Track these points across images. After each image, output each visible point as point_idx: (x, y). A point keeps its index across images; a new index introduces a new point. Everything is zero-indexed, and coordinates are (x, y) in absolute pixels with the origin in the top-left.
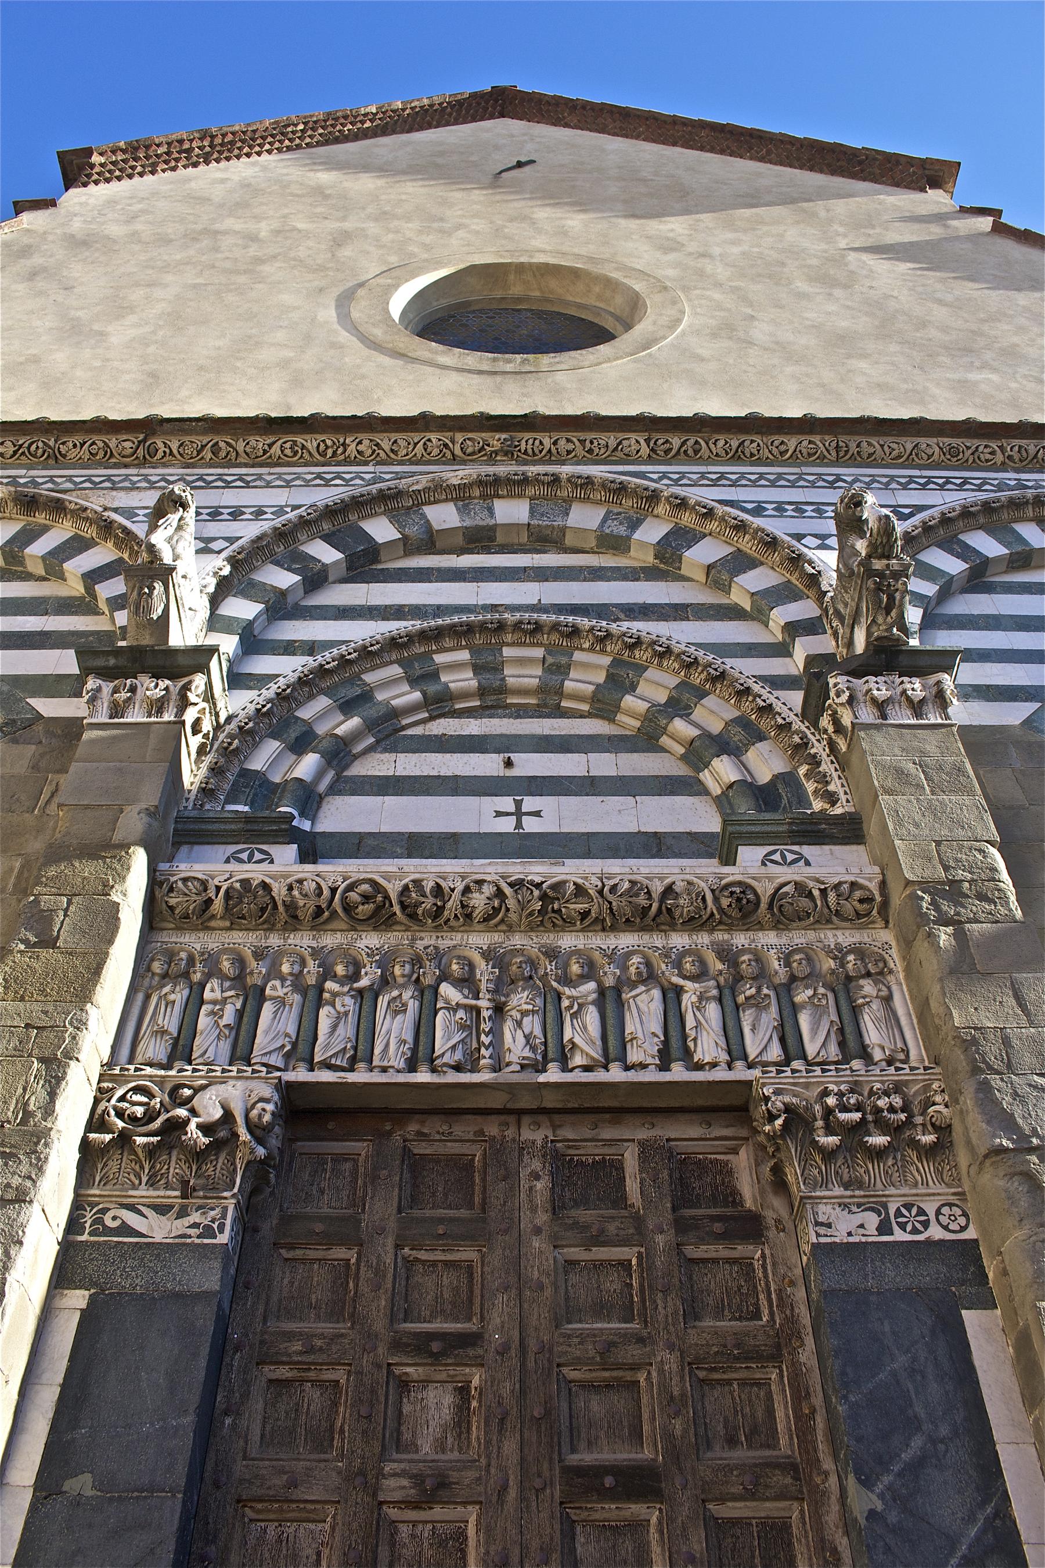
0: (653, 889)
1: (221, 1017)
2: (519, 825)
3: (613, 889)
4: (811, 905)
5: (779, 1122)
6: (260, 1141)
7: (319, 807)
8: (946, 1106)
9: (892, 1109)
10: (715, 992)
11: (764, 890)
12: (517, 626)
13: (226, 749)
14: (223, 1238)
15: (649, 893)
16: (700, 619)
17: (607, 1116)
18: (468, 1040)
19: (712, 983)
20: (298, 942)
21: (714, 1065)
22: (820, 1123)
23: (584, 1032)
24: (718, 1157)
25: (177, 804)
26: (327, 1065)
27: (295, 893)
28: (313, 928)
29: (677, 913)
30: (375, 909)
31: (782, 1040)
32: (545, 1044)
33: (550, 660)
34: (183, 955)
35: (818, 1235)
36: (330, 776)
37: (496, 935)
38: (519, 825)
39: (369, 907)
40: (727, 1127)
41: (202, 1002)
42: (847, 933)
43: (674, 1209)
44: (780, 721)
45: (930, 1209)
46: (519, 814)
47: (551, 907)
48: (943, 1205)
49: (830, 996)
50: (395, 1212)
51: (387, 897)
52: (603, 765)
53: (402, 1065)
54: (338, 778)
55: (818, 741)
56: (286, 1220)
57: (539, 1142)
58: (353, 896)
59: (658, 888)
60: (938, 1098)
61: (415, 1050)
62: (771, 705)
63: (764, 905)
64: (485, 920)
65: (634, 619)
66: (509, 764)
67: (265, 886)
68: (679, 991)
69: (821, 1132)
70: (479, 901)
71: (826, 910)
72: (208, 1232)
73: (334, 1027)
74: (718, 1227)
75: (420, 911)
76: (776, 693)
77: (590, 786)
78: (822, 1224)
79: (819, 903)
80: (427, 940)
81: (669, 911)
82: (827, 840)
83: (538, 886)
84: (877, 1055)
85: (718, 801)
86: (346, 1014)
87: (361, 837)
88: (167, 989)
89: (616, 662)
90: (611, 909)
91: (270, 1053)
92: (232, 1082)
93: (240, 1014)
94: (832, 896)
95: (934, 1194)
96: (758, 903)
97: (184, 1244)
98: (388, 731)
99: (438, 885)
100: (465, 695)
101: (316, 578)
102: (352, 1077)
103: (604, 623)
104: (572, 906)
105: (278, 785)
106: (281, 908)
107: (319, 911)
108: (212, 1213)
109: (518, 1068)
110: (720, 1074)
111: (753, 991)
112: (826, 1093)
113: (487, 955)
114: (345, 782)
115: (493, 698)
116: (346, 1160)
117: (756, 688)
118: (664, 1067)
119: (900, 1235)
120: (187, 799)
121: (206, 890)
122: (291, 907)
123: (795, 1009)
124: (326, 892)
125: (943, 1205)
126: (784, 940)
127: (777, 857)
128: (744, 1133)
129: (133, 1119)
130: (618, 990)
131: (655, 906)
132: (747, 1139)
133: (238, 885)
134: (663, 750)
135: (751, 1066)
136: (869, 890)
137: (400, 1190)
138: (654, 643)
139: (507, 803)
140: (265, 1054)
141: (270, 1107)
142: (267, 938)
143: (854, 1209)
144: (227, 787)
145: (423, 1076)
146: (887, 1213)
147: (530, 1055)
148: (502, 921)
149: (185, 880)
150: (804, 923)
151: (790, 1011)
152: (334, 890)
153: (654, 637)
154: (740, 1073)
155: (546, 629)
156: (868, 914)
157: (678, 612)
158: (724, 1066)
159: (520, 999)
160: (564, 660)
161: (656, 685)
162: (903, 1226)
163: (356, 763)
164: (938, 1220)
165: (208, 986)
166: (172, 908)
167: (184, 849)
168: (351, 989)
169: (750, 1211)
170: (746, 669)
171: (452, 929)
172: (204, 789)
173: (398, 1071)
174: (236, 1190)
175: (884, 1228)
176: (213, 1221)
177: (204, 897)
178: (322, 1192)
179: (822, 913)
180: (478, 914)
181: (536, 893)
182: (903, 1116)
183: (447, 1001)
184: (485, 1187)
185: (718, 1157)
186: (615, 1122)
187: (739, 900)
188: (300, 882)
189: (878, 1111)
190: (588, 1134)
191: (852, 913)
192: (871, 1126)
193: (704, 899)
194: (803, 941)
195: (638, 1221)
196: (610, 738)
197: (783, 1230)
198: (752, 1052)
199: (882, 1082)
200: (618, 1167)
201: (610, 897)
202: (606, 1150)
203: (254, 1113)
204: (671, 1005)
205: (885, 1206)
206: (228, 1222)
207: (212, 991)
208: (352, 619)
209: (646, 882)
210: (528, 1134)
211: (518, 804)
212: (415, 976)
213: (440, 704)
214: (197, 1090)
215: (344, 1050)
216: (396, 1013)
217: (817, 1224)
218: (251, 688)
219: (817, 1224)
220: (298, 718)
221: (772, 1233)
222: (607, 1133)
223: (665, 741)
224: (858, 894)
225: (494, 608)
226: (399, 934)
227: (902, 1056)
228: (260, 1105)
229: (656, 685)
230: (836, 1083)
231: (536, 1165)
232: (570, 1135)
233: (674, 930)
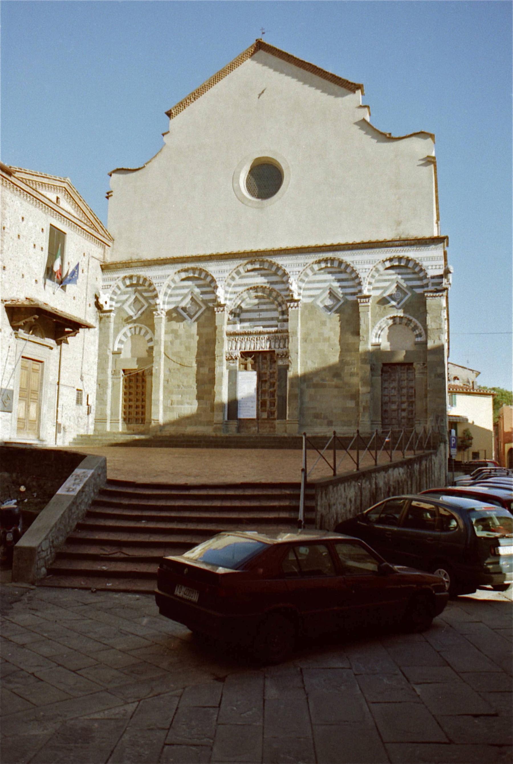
77: (267, 310)
110: (273, 350)
139: (258, 313)
161: (274, 294)
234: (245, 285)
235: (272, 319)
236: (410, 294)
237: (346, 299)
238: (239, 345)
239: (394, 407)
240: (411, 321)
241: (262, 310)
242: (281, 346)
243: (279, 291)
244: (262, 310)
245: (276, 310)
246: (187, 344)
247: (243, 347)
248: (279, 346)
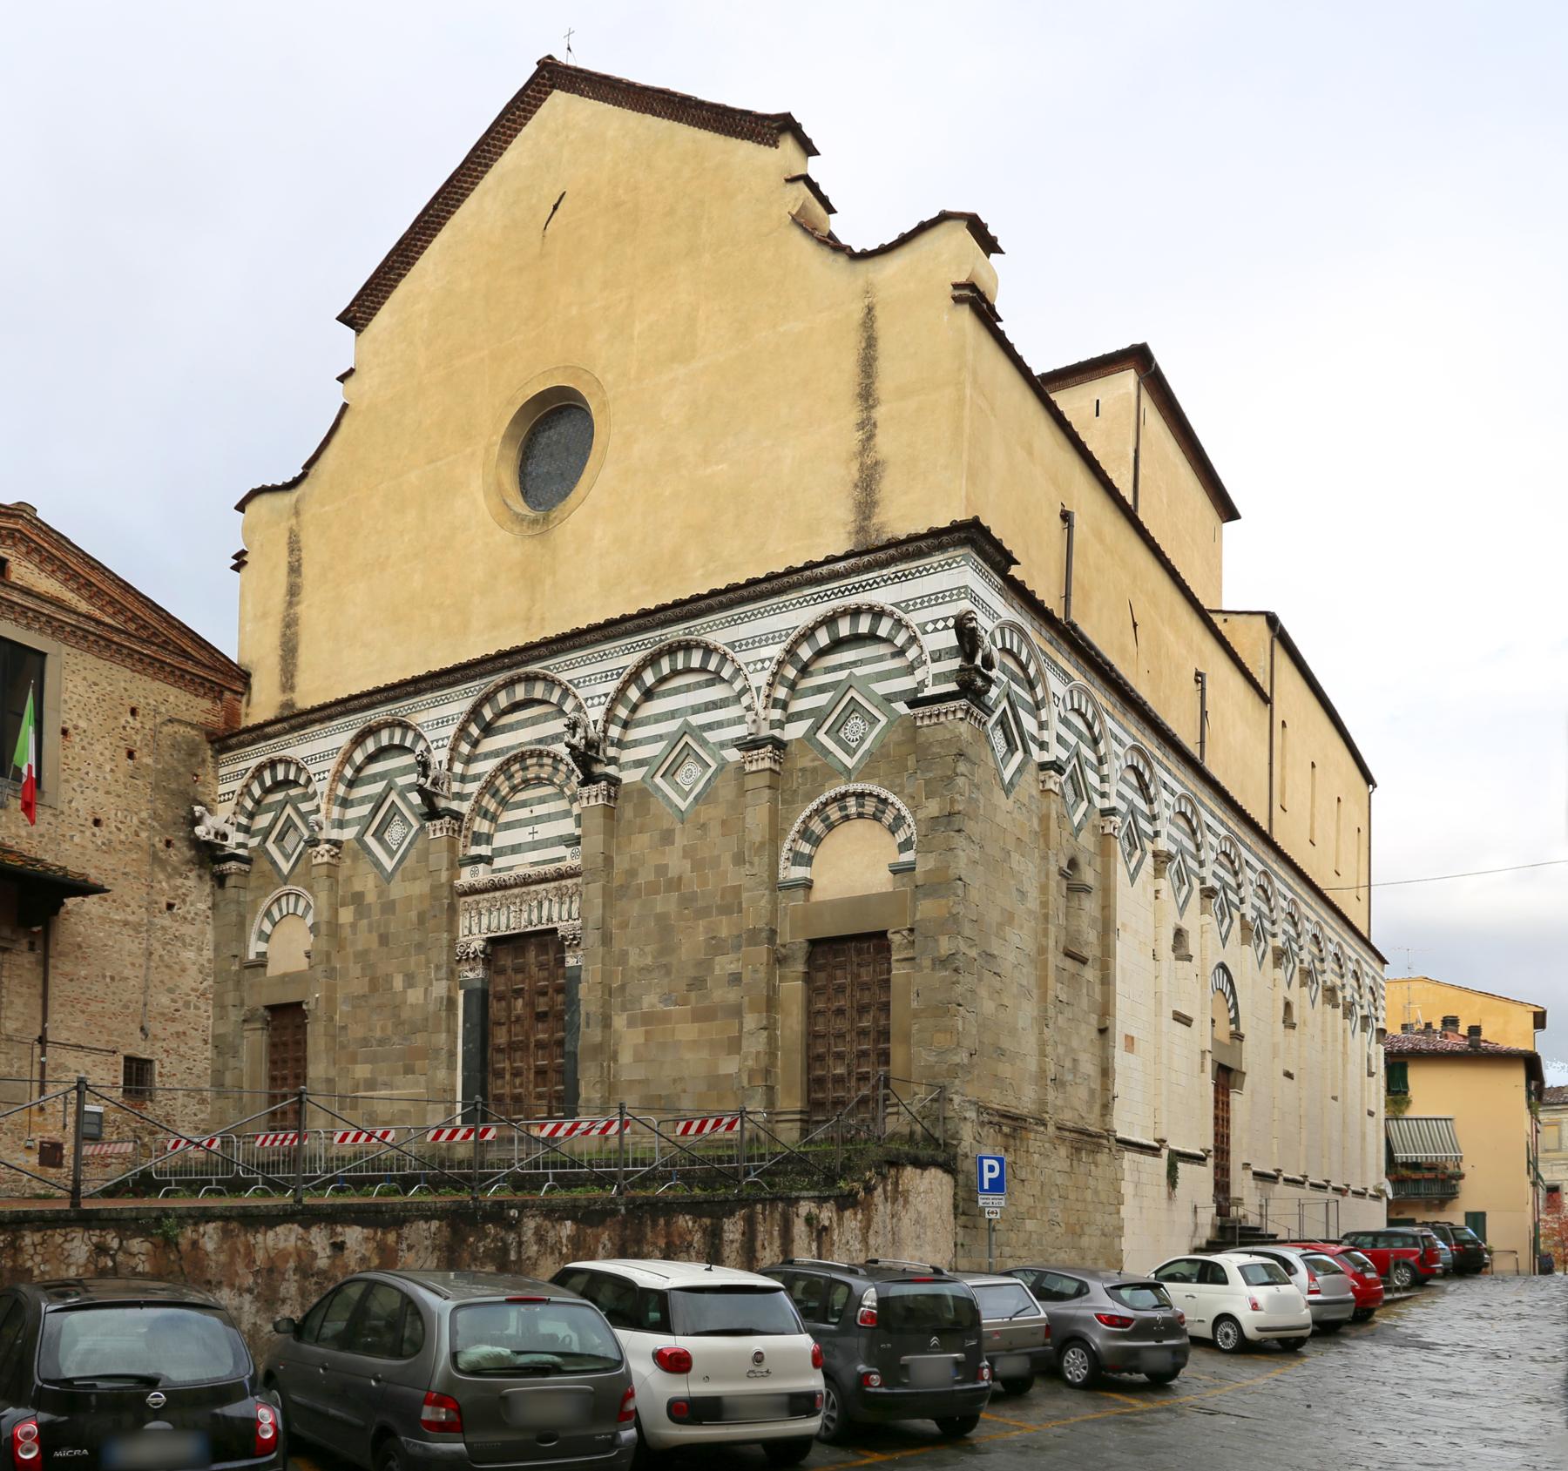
77: (549, 818)
98: (504, 803)
101: (475, 744)
213: (514, 789)
225: (521, 745)
236: (883, 721)
237: (723, 759)
239: (840, 1070)
240: (884, 801)
241: (539, 820)
244: (539, 820)
245: (567, 814)
246: (382, 930)
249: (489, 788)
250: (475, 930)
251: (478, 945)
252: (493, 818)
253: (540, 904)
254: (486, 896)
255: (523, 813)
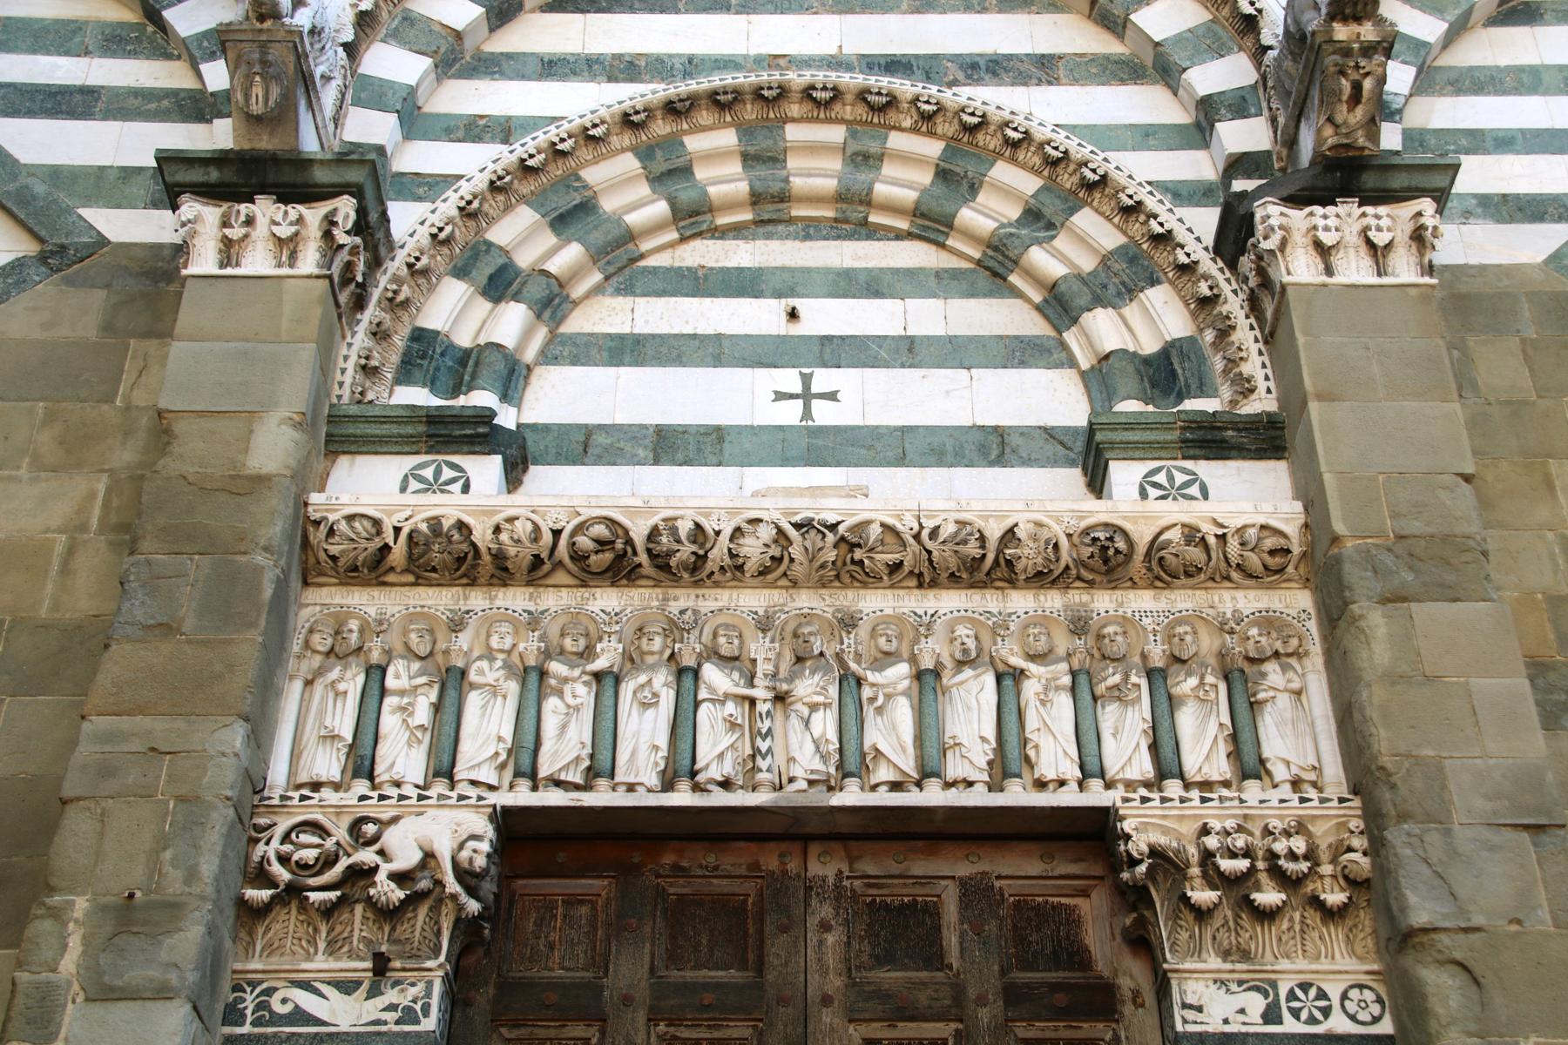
0: (987, 533)
1: (411, 714)
2: (807, 413)
3: (934, 533)
4: (1203, 557)
5: (1142, 868)
6: (472, 892)
7: (526, 384)
8: (1365, 854)
9: (1292, 856)
10: (1066, 680)
11: (1142, 535)
12: (808, 92)
13: (391, 300)
14: (430, 1024)
15: (982, 539)
16: (1075, 81)
17: (920, 844)
18: (739, 744)
19: (1064, 666)
20: (508, 604)
21: (1062, 783)
22: (1195, 871)
23: (892, 734)
24: (1064, 900)
25: (329, 396)
26: (558, 783)
27: (504, 537)
28: (529, 583)
29: (1019, 566)
30: (613, 558)
31: (1154, 748)
32: (841, 750)
33: (853, 147)
34: (354, 625)
35: (1185, 1021)
36: (542, 334)
37: (776, 592)
38: (807, 413)
39: (608, 556)
40: (1076, 861)
41: (383, 692)
42: (1252, 594)
43: (1003, 972)
44: (1183, 259)
45: (1334, 991)
46: (807, 396)
47: (851, 557)
48: (1352, 987)
49: (1223, 687)
50: (646, 976)
51: (629, 542)
52: (927, 317)
53: (653, 780)
54: (553, 335)
55: (1235, 292)
56: (507, 987)
57: (831, 880)
58: (584, 542)
59: (994, 532)
60: (1356, 842)
61: (672, 757)
62: (1170, 232)
63: (1139, 556)
64: (761, 574)
65: (979, 82)
66: (793, 315)
67: (461, 526)
68: (1019, 675)
69: (1198, 882)
70: (754, 548)
71: (1223, 565)
72: (409, 1016)
73: (564, 728)
74: (1061, 999)
75: (673, 562)
76: (1181, 212)
77: (908, 351)
78: (1191, 1007)
79: (1214, 555)
80: (683, 600)
81: (1009, 563)
82: (1233, 453)
83: (833, 527)
84: (1280, 772)
85: (1083, 375)
86: (577, 709)
87: (588, 431)
88: (334, 674)
89: (951, 151)
90: (930, 561)
91: (479, 765)
92: (431, 812)
93: (437, 708)
94: (1233, 545)
95: (1340, 972)
96: (1129, 556)
97: (379, 1033)
98: (620, 261)
99: (698, 526)
100: (731, 206)
102: (589, 799)
103: (934, 89)
104: (878, 557)
105: (467, 353)
106: (487, 558)
107: (537, 561)
108: (413, 991)
109: (804, 785)
110: (1069, 797)
111: (1117, 679)
112: (1205, 831)
113: (764, 624)
114: (563, 344)
115: (771, 209)
116: (581, 902)
117: (1151, 204)
118: (994, 787)
119: (1290, 1026)
120: (341, 384)
121: (379, 533)
122: (499, 557)
123: (1173, 703)
124: (547, 537)
125: (1352, 987)
126: (1162, 604)
127: (1161, 478)
128: (1097, 869)
129: (306, 866)
130: (936, 673)
131: (991, 557)
132: (1101, 878)
133: (424, 527)
134: (1016, 293)
135: (1109, 786)
136: (1285, 536)
137: (653, 944)
138: (1007, 124)
139: (789, 379)
140: (473, 767)
141: (485, 847)
142: (466, 598)
143: (1234, 987)
144: (395, 359)
145: (682, 797)
146: (1277, 995)
147: (821, 767)
148: (785, 574)
149: (350, 518)
150: (1190, 581)
151: (1165, 705)
152: (557, 533)
153: (1006, 115)
154: (1095, 796)
155: (849, 98)
156: (1281, 570)
157: (1043, 69)
158: (1074, 786)
159: (807, 687)
160: (873, 147)
161: (1008, 189)
162: (1296, 1013)
163: (576, 313)
164: (1343, 1006)
165: (391, 671)
166: (334, 558)
167: (343, 462)
168: (584, 672)
169: (1101, 978)
170: (1139, 170)
171: (717, 585)
172: (364, 367)
173: (650, 791)
174: (442, 958)
175: (1271, 1015)
176: (414, 1001)
177: (378, 543)
178: (552, 947)
179: (1217, 569)
180: (751, 567)
181: (831, 538)
182: (1304, 866)
183: (711, 689)
184: (762, 941)
185: (1064, 900)
186: (931, 853)
187: (1104, 549)
188: (511, 520)
189: (1272, 856)
190: (895, 869)
191: (1261, 568)
192: (1263, 878)
193: (1056, 546)
194: (1189, 605)
195: (958, 991)
196: (939, 274)
197: (1142, 1005)
198: (1112, 769)
199: (1281, 818)
200: (931, 913)
201: (929, 545)
202: (918, 890)
203: (465, 854)
204: (1009, 698)
205: (1274, 984)
206: (435, 1002)
207: (397, 676)
208: (563, 77)
209: (980, 523)
210: (815, 868)
211: (806, 380)
212: (668, 653)
213: (693, 218)
214: (384, 824)
215: (578, 759)
216: (645, 706)
217: (1185, 1006)
218: (420, 199)
219: (1185, 1006)
220: (490, 245)
221: (1128, 1009)
222: (920, 867)
223: (1014, 279)
224: (1270, 542)
225: (773, 61)
226: (646, 592)
227: (1312, 776)
228: (472, 844)
229: (1008, 189)
230: (1218, 817)
231: (826, 911)
232: (871, 869)
233: (1015, 588)
234: (625, 68)
235: (995, 446)
238: (487, 726)
242: (1202, 741)
243: (1079, 149)
245: (1017, 353)
247: (565, 741)
248: (1166, 765)
249: (550, 177)
250: (402, 757)
251: (444, 831)
252: (552, 301)
253: (927, 681)
254: (515, 599)
255: (757, 317)
